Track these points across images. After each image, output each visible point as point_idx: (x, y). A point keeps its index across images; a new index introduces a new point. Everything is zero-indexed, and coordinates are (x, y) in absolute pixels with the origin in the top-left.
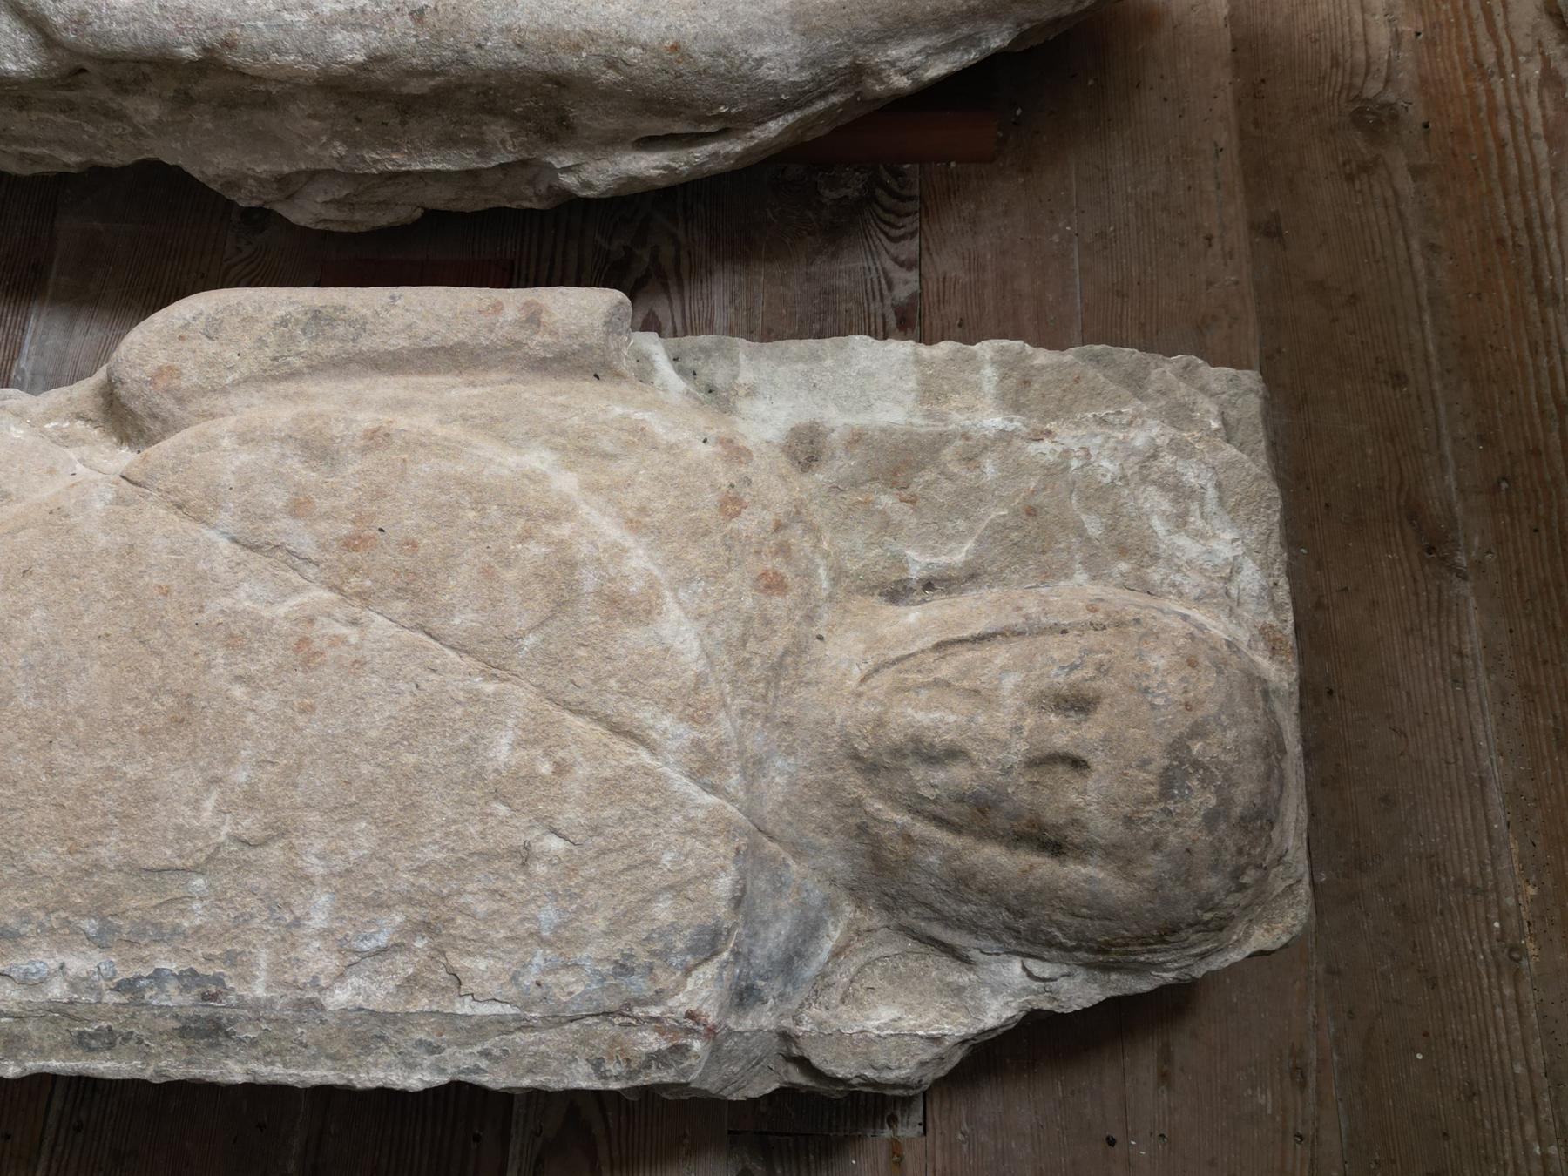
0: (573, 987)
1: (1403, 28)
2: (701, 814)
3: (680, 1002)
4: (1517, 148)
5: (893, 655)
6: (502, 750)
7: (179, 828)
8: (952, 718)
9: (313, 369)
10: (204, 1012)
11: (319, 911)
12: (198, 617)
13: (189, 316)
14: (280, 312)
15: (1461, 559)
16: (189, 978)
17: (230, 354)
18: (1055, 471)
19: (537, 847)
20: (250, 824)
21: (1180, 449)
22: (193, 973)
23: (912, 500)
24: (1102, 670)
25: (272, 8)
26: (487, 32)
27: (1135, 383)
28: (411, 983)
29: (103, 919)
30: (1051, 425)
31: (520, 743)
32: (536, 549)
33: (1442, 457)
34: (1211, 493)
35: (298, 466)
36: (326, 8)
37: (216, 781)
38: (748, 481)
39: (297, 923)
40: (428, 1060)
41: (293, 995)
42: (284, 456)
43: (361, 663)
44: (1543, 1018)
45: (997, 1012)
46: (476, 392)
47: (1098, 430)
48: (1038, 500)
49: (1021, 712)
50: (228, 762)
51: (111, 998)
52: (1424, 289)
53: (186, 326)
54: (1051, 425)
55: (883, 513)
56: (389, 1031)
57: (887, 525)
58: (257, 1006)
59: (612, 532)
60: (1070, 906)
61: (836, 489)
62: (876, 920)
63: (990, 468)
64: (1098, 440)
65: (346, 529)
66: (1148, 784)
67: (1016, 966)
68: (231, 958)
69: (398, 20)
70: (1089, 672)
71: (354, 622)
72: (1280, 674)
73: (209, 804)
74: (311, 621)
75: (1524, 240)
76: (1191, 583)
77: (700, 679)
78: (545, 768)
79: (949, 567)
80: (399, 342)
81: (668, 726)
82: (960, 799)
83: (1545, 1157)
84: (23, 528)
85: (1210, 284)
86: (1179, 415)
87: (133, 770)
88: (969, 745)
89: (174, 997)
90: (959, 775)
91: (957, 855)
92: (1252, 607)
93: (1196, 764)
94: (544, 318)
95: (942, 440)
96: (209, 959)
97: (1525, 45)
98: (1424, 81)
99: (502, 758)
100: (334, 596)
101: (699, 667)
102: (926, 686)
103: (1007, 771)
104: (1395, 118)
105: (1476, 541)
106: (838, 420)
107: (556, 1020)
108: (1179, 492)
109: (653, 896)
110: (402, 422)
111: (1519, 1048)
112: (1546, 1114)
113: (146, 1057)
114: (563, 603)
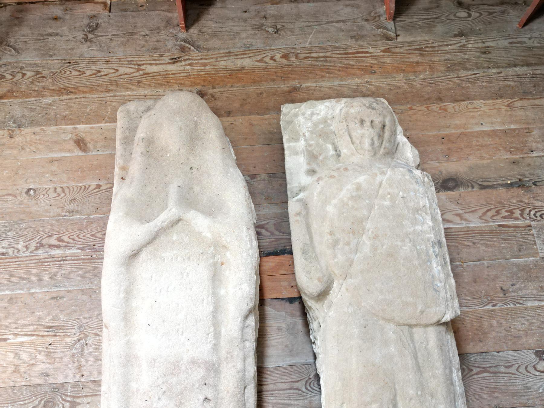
0: (421, 189)
1: (177, 89)
2: (392, 173)
3: (420, 175)
4: (208, 71)
5: (355, 151)
6: (387, 203)
7: (410, 252)
8: (367, 140)
9: (314, 252)
10: (437, 244)
11: (419, 228)
12: (372, 257)
13: (306, 278)
14: (303, 260)
15: (298, 85)
16: (433, 247)
17: (314, 268)
18: (311, 132)
19: (402, 196)
20: (407, 240)
21: (304, 114)
22: (432, 246)
23: (320, 154)
24: (356, 118)
25: (249, 257)
26: (249, 218)
27: (290, 122)
28: (426, 213)
29: (427, 262)
30: (301, 134)
31: (385, 201)
32: (350, 203)
33: (278, 87)
34: (312, 110)
35: (339, 246)
36: (249, 246)
37: (401, 247)
38: (326, 176)
39: (421, 231)
40: (436, 210)
41: (432, 230)
42: (338, 249)
43: (376, 228)
44: (377, 79)
45: (405, 139)
46: (314, 223)
47: (301, 127)
48: (318, 135)
49: (365, 130)
50: (398, 246)
51: (439, 259)
52: (241, 88)
53: (308, 278)
54: (301, 134)
55: (323, 159)
56: (434, 216)
57: (326, 158)
58: (435, 236)
59: (344, 192)
60: (391, 125)
61: (319, 166)
62: (396, 156)
63: (312, 142)
64: (304, 126)
65: (351, 235)
66: (374, 112)
67: (398, 136)
68: (429, 241)
69: (250, 233)
70: (356, 121)
71: (368, 230)
72: (344, 100)
73: (405, 248)
74: (369, 238)
75: (230, 72)
76: (330, 112)
77: (369, 175)
78: (389, 196)
79: (332, 147)
80: (307, 237)
81: (379, 178)
82: (379, 139)
83: (398, 80)
84: (359, 294)
85: (242, 124)
86: (296, 115)
87: (402, 261)
88: (371, 137)
89: (436, 249)
90: (376, 139)
91: (386, 141)
92: (332, 104)
93: (370, 105)
94: (298, 212)
95: (307, 150)
96: (429, 244)
97: (182, 68)
98: (191, 86)
99: (389, 203)
100: (364, 235)
101: (367, 176)
102: (361, 145)
103: (374, 132)
104: (200, 91)
105: (295, 83)
106: (305, 167)
107: (426, 192)
108: (312, 114)
109: (405, 178)
110: (327, 230)
111: (382, 83)
112: (391, 80)
113: (446, 253)
114: (359, 197)
